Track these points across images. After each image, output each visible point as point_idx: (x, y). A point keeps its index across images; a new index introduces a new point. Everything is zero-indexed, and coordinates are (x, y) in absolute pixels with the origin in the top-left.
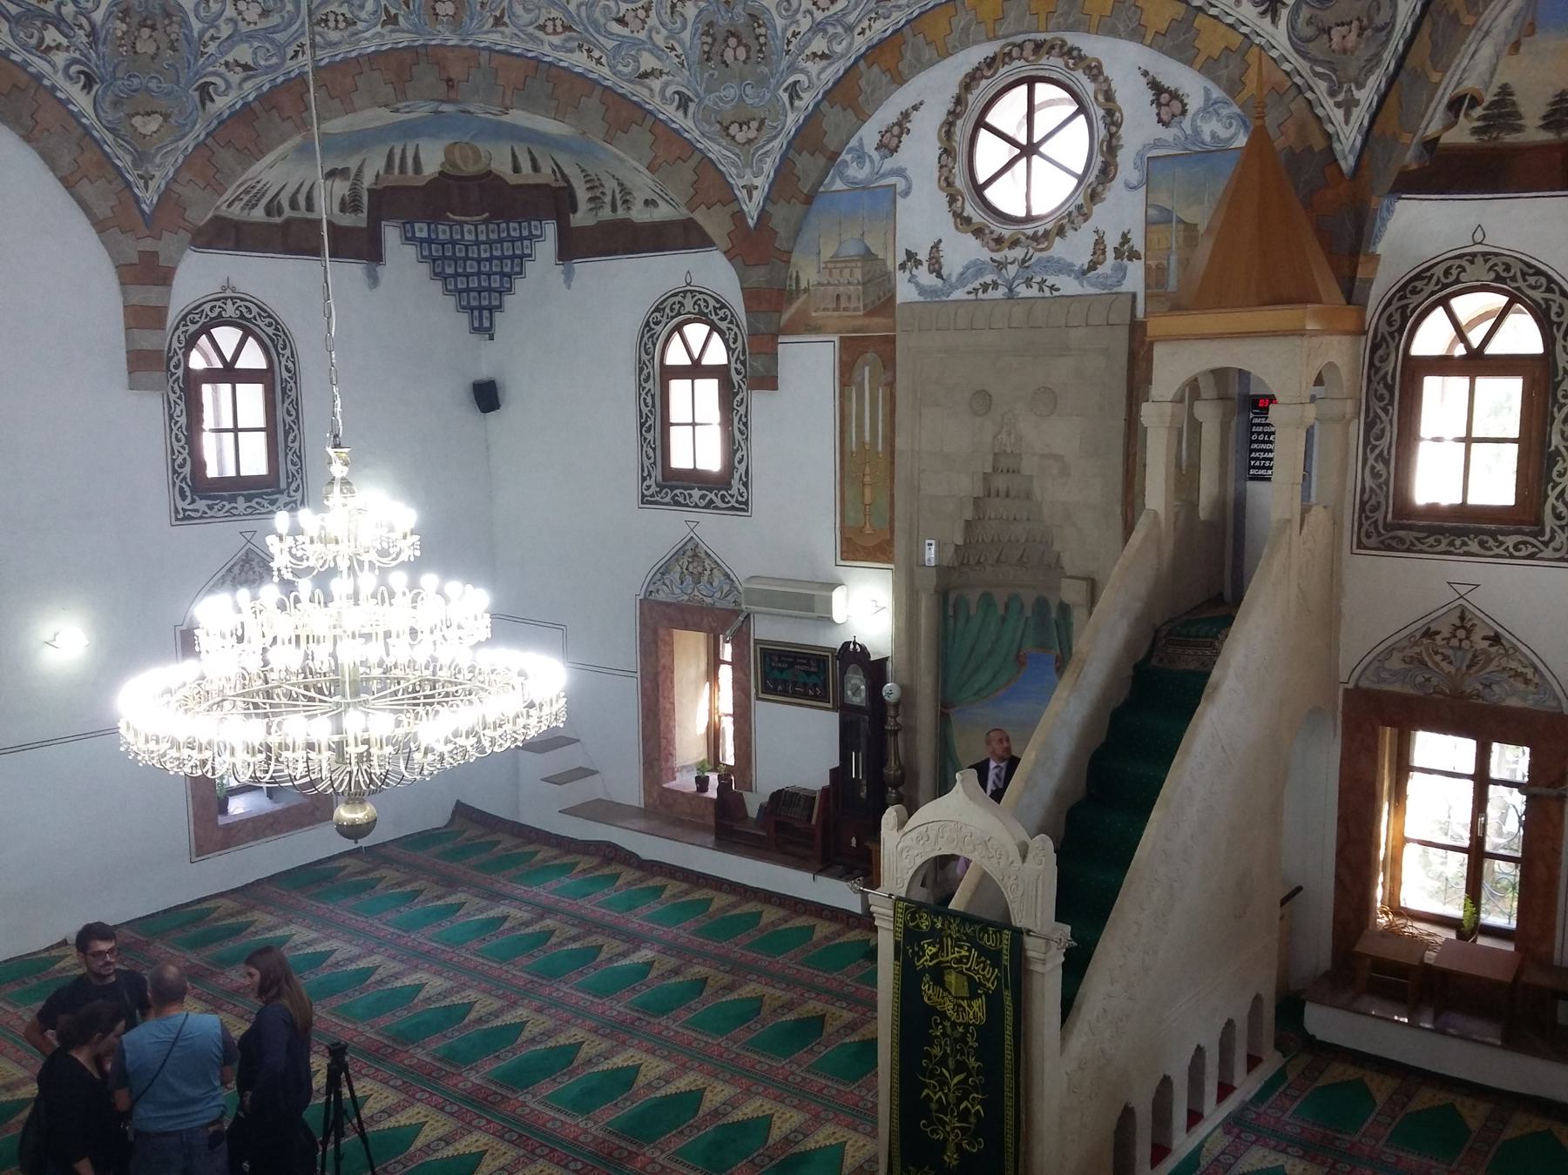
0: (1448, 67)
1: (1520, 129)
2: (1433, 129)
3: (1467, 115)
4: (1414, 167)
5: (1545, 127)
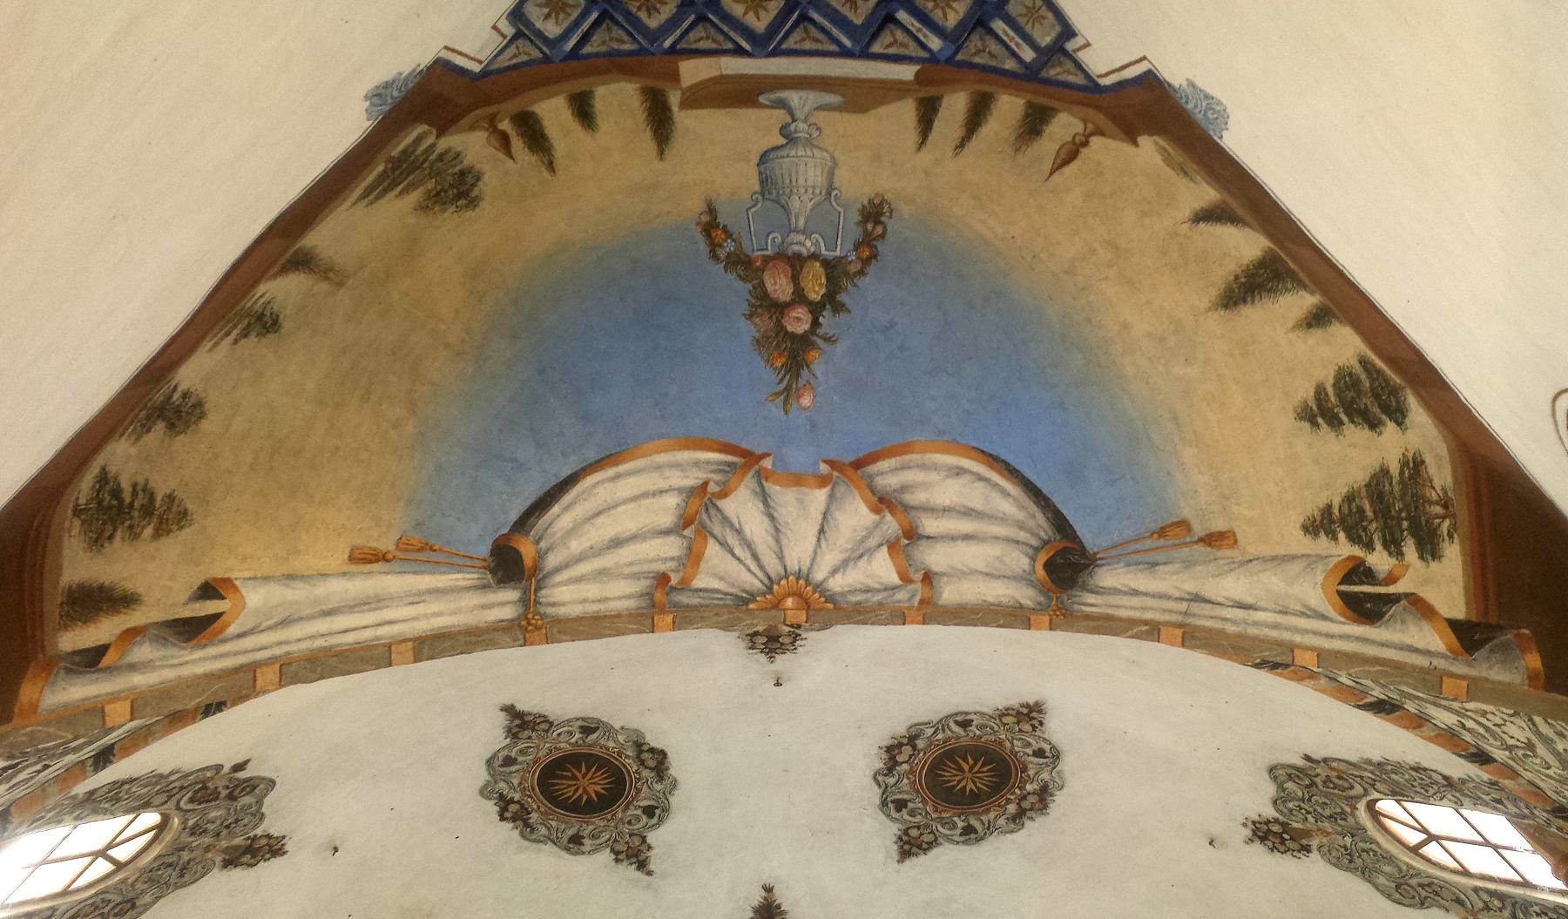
0: (1279, 644)
1: (1414, 467)
2: (1430, 639)
3: (1391, 579)
4: (1534, 661)
5: (1398, 415)
